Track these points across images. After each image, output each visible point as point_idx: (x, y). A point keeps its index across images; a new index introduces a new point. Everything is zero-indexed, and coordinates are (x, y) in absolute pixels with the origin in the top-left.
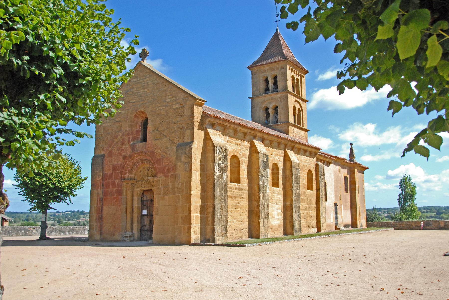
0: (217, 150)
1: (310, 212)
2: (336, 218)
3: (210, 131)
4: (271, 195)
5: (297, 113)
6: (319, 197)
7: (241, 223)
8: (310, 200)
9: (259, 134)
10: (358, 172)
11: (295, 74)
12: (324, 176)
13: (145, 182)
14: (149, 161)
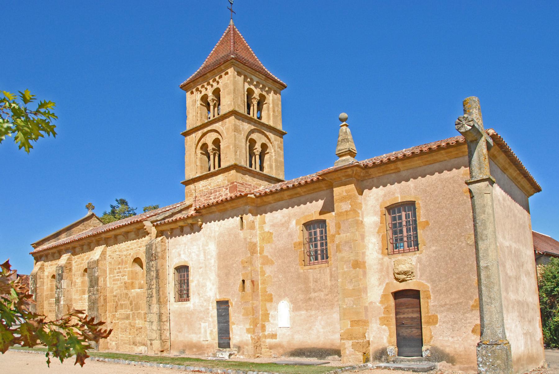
1: (137, 322)
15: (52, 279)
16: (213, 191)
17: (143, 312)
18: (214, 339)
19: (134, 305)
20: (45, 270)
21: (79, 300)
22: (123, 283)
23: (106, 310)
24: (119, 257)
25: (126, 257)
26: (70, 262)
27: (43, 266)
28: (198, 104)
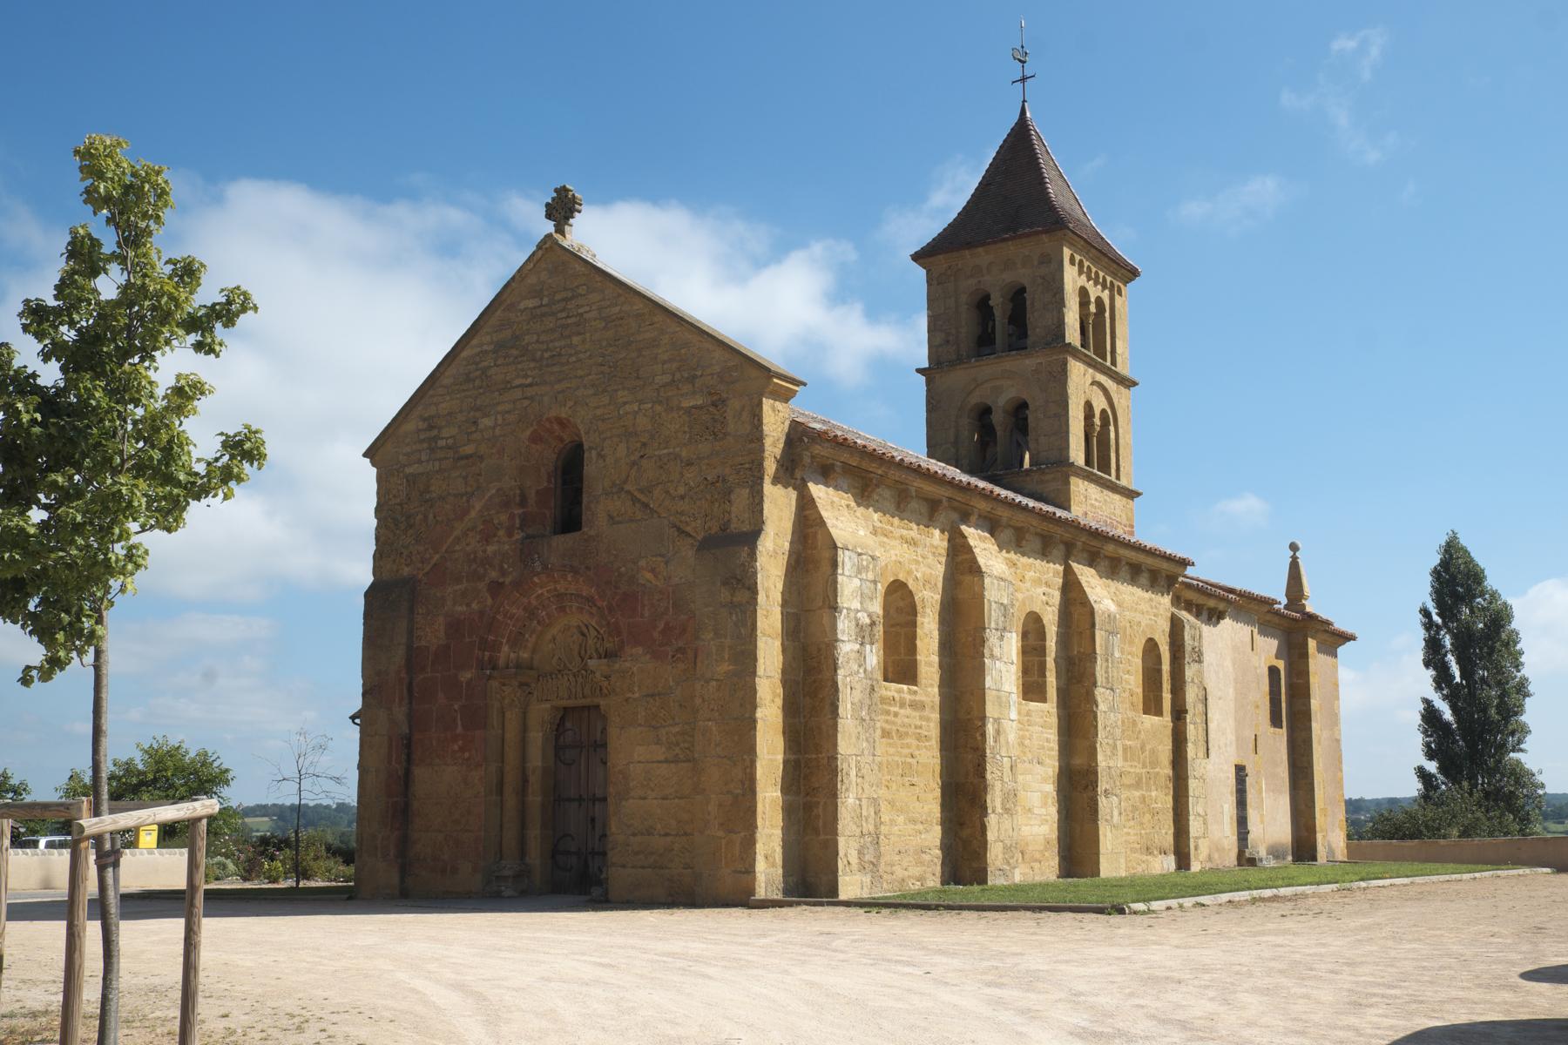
0: (846, 560)
1: (1154, 794)
2: (1242, 821)
3: (818, 491)
5: (1098, 429)
6: (1185, 740)
7: (920, 827)
8: (1153, 751)
9: (983, 506)
10: (1319, 650)
11: (1091, 282)
12: (1200, 661)
13: (571, 678)
14: (590, 600)
19: (1147, 752)
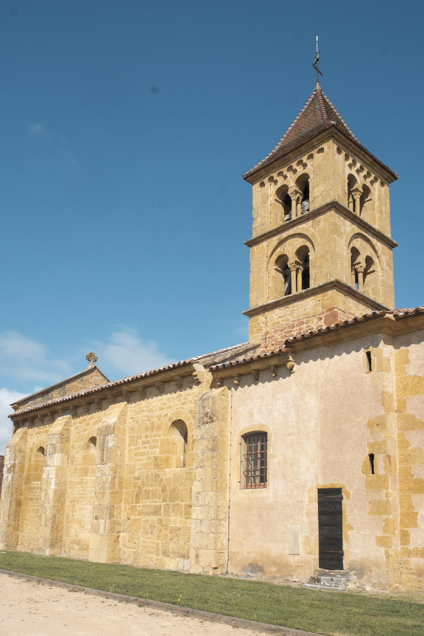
1: (172, 518)
4: (83, 490)
15: (37, 453)
16: (296, 323)
17: (183, 504)
18: (311, 553)
19: (168, 492)
20: (28, 440)
21: (78, 484)
22: (152, 459)
23: (122, 500)
24: (148, 419)
25: (159, 419)
26: (69, 427)
27: (26, 434)
28: (272, 200)
